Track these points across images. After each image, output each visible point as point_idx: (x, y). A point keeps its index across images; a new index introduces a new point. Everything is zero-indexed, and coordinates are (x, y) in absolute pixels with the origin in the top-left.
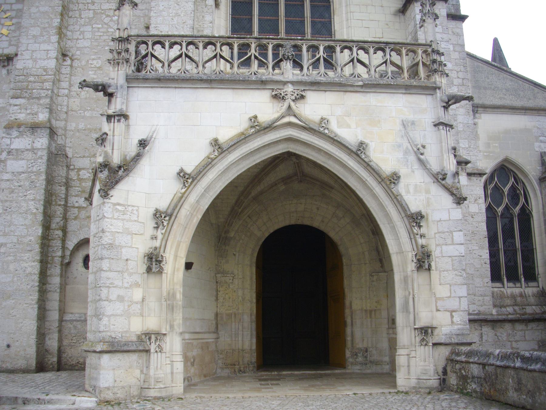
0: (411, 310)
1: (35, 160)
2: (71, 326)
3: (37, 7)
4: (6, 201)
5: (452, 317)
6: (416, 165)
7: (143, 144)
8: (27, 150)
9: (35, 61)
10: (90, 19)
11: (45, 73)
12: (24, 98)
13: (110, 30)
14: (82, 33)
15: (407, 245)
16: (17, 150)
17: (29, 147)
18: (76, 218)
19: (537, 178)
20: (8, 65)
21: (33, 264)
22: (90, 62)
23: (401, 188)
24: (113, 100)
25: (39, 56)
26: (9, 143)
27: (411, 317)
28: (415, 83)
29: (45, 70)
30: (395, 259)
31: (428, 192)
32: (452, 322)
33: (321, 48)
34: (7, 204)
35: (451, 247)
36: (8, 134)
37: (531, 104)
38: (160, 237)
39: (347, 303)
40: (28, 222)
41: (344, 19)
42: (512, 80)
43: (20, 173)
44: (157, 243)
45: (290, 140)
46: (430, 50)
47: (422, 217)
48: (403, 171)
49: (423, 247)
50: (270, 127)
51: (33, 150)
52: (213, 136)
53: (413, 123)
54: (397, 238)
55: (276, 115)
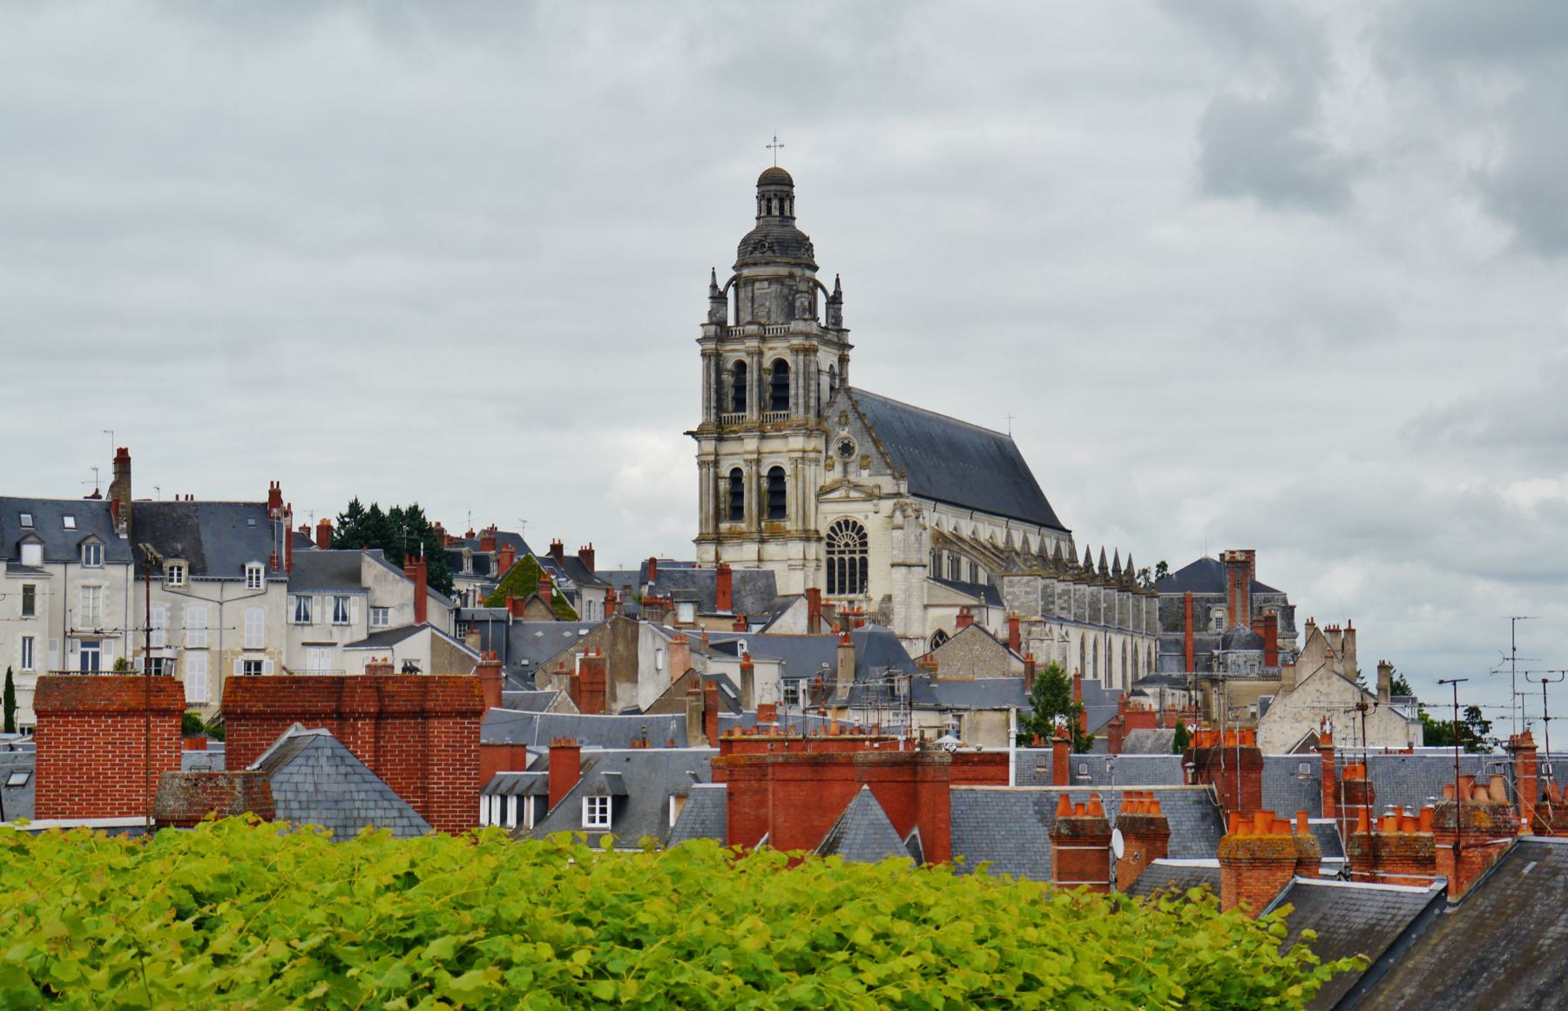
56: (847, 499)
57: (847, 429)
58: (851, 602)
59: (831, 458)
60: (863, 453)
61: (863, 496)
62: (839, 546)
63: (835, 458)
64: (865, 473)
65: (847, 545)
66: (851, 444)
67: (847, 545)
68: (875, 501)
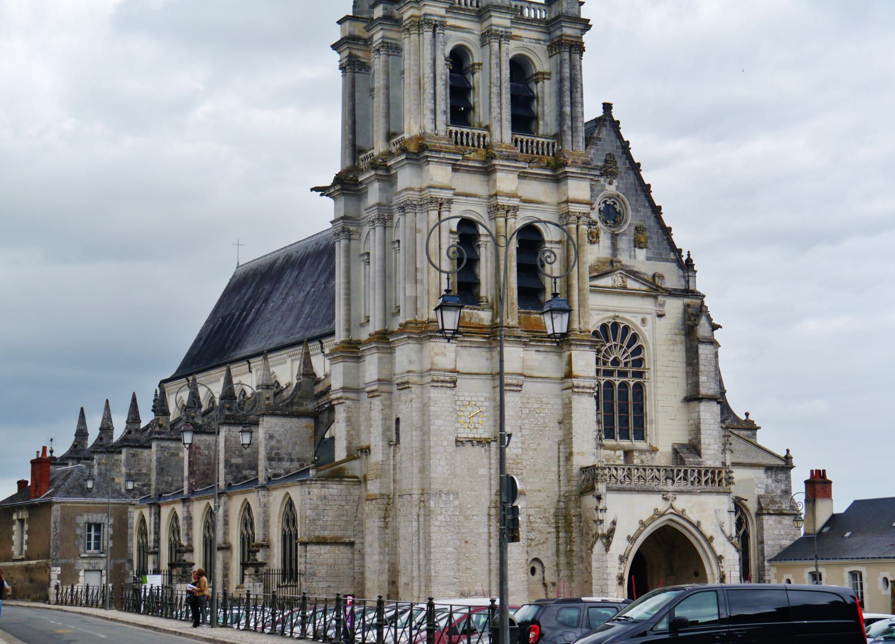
6: (720, 532)
7: (614, 523)
11: (517, 458)
13: (539, 423)
19: (755, 512)
22: (530, 445)
23: (714, 544)
24: (601, 501)
28: (721, 490)
29: (517, 456)
31: (724, 545)
33: (682, 471)
37: (754, 461)
38: (623, 568)
41: (653, 405)
42: (744, 444)
44: (622, 572)
45: (670, 520)
46: (728, 471)
47: (723, 558)
50: (662, 515)
52: (640, 519)
53: (719, 510)
55: (665, 508)
56: (623, 291)
57: (615, 182)
58: (628, 453)
60: (638, 223)
61: (645, 288)
62: (605, 363)
64: (641, 254)
65: (616, 362)
66: (618, 207)
67: (616, 362)
68: (661, 299)
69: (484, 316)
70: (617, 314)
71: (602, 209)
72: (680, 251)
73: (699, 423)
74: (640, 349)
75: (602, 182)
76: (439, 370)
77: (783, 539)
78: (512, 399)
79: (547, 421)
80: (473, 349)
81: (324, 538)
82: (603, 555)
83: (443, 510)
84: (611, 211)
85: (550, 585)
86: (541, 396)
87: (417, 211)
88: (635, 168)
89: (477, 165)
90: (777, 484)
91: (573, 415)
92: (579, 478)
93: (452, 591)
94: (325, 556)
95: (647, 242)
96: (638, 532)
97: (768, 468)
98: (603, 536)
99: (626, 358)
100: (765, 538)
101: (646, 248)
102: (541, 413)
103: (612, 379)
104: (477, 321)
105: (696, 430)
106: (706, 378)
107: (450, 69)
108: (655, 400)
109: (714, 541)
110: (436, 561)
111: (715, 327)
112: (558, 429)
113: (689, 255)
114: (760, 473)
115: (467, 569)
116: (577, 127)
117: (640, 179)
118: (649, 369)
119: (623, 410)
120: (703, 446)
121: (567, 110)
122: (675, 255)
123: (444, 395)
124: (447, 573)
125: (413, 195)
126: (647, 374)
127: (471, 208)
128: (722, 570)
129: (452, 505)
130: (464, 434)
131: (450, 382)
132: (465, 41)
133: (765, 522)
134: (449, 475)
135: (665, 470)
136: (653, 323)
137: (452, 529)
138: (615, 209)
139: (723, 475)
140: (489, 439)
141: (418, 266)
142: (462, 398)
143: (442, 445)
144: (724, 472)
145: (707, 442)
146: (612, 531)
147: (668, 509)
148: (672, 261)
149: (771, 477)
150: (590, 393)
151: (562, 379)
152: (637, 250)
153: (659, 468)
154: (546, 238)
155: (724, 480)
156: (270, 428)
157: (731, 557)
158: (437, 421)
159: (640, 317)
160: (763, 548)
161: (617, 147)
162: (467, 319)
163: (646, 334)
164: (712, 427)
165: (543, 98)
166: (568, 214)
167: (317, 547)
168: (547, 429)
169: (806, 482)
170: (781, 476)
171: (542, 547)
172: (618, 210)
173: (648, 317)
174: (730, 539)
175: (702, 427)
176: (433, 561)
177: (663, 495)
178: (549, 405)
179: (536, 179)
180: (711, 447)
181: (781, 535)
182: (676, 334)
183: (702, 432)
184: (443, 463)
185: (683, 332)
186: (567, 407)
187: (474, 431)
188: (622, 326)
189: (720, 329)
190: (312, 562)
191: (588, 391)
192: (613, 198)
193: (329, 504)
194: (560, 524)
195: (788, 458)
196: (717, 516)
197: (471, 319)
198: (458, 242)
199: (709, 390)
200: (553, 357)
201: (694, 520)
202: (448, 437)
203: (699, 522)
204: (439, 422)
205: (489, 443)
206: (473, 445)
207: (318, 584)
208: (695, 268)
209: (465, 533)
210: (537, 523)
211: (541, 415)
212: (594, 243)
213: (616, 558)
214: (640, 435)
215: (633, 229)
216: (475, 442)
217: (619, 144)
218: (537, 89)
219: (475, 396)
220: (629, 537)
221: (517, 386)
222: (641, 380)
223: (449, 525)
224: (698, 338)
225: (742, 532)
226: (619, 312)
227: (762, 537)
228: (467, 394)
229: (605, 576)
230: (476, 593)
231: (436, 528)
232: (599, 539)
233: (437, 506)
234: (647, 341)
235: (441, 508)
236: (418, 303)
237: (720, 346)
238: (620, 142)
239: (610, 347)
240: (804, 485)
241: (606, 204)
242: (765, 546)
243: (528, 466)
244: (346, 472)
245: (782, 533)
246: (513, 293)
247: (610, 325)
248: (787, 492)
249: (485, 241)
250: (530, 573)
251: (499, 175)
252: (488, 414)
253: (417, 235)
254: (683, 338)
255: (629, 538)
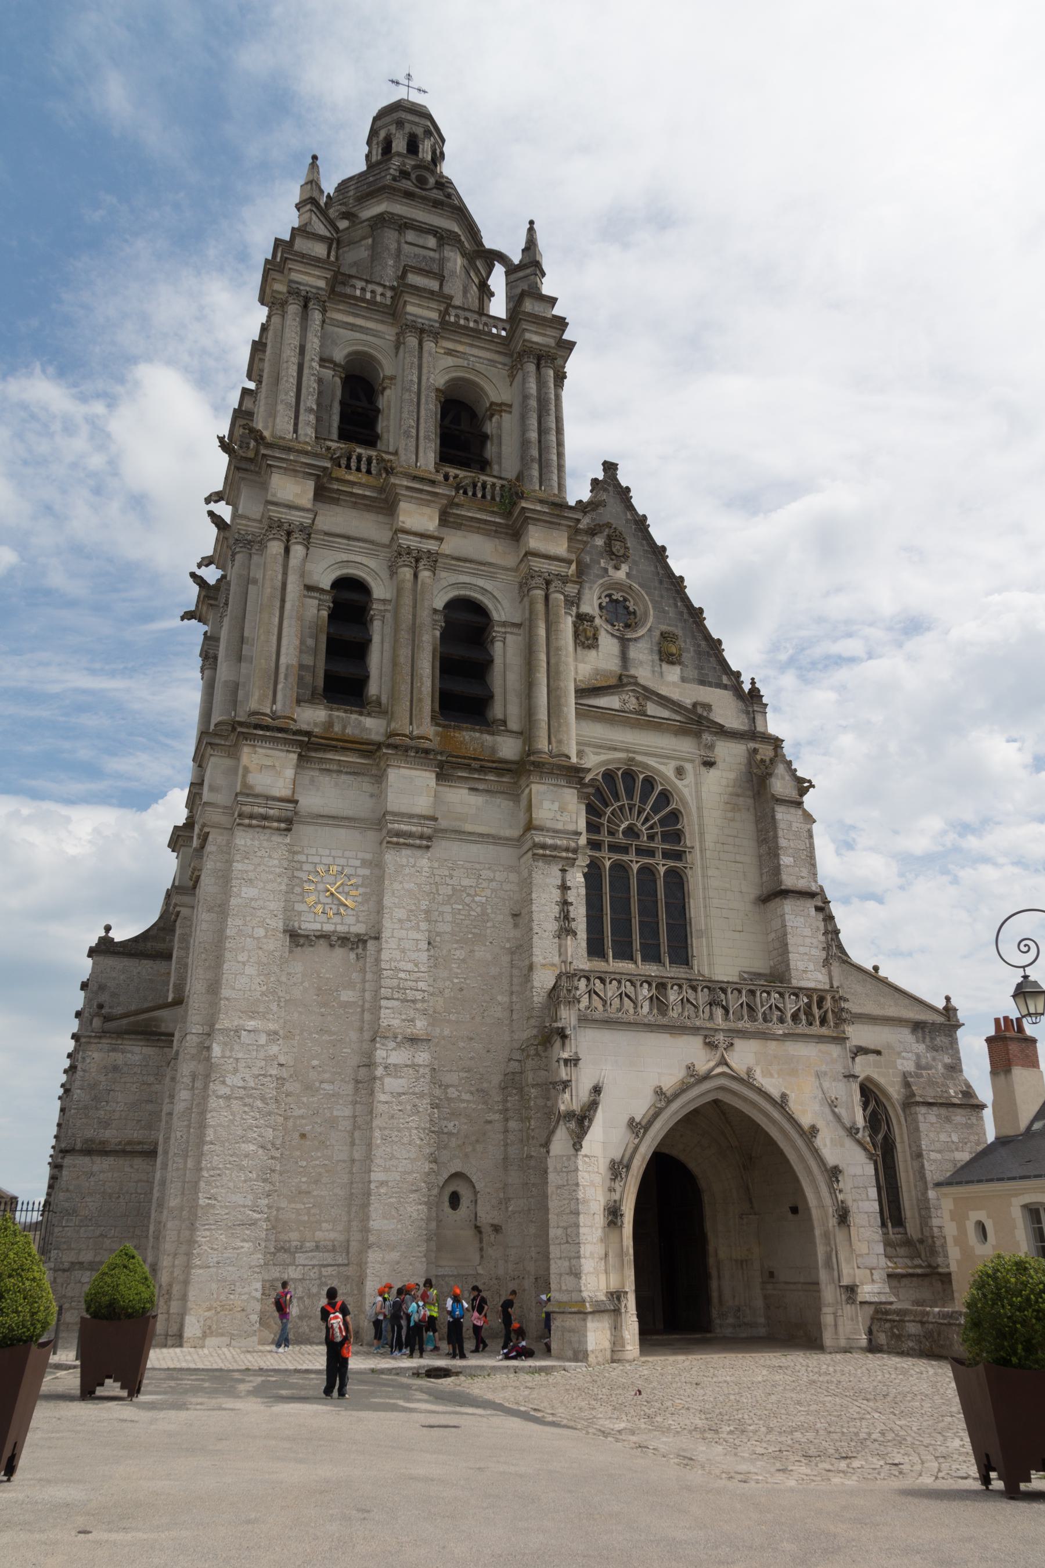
0: (835, 1267)
1: (417, 1079)
2: (443, 1283)
3: (401, 883)
4: (385, 1128)
5: (872, 1274)
7: (597, 1090)
8: (407, 1066)
9: (403, 951)
10: (450, 897)
12: (397, 999)
13: (472, 913)
14: (441, 913)
15: (828, 1201)
16: (395, 1065)
17: (409, 1063)
18: (445, 1147)
20: (358, 947)
21: (420, 1207)
22: (453, 952)
23: (819, 1142)
24: (567, 1042)
25: (407, 947)
26: (385, 1055)
27: (836, 1273)
30: (815, 1213)
31: (842, 1146)
32: (873, 1280)
34: (386, 1132)
35: (867, 1203)
36: (383, 1045)
38: (619, 1189)
39: (711, 1248)
40: (413, 1156)
43: (400, 1094)
44: (617, 1197)
45: (722, 1088)
46: (837, 996)
48: (820, 1125)
49: (842, 1202)
50: (707, 1077)
51: (413, 1066)
54: (817, 1192)
55: (712, 1064)
56: (641, 721)
57: (625, 568)
59: (591, 619)
61: (678, 718)
63: (598, 621)
64: (673, 673)
65: (630, 831)
68: (707, 737)
69: (372, 726)
70: (631, 755)
71: (604, 604)
72: (738, 674)
73: (785, 934)
74: (675, 816)
75: (603, 565)
76: (257, 796)
77: (957, 1149)
78: (412, 860)
79: (489, 911)
80: (343, 777)
81: (103, 1143)
82: (569, 1158)
83: (242, 1065)
84: (621, 611)
85: (490, 1229)
86: (477, 866)
87: (254, 551)
88: (659, 553)
89: (368, 493)
90: (935, 1053)
91: (534, 896)
92: (547, 1011)
93: (244, 1240)
94: (102, 1176)
95: (680, 655)
96: (651, 1112)
97: (918, 1027)
98: (570, 1115)
99: (651, 827)
100: (924, 1147)
101: (680, 663)
102: (476, 895)
103: (625, 858)
104: (357, 732)
105: (782, 948)
106: (791, 859)
107: (341, 378)
108: (704, 898)
109: (819, 1137)
110: (212, 1173)
111: (803, 786)
112: (511, 926)
113: (753, 683)
114: (905, 1035)
115: (300, 1193)
116: (548, 460)
117: (667, 568)
118: (693, 848)
119: (649, 910)
120: (793, 973)
121: (533, 435)
122: (730, 679)
123: (265, 844)
124: (238, 1199)
125: (246, 525)
126: (689, 857)
127: (358, 559)
128: (840, 1197)
129: (262, 1055)
130: (310, 924)
131: (279, 820)
132: (370, 347)
133: (921, 1118)
134: (263, 994)
135: (708, 988)
136: (695, 775)
137: (259, 1103)
138: (627, 608)
139: (828, 1004)
140: (365, 935)
141: (246, 634)
142: (316, 859)
143: (251, 936)
144: (829, 998)
145: (801, 966)
146: (592, 1106)
147: (717, 1065)
148: (725, 687)
149: (924, 1042)
150: (567, 858)
151: (518, 840)
152: (665, 666)
153: (695, 983)
154: (495, 616)
155: (830, 1015)
156: (102, 972)
157: (858, 1171)
158: (244, 889)
159: (673, 764)
160: (922, 1166)
161: (627, 521)
162: (337, 728)
163: (686, 791)
164: (808, 941)
165: (500, 437)
166: (531, 575)
167: (87, 1160)
168: (489, 924)
169: (989, 1040)
170: (941, 1040)
171: (474, 1150)
172: (631, 609)
173: (688, 766)
174: (852, 1131)
175: (791, 940)
176: (205, 1174)
177: (706, 1037)
178: (494, 883)
179: (478, 531)
180: (809, 975)
181: (953, 1142)
182: (738, 795)
183: (791, 949)
184: (250, 970)
185: (749, 793)
186: (526, 885)
187: (337, 919)
188: (641, 777)
189: (811, 790)
190: (71, 1188)
191: (564, 854)
192: (623, 591)
193: (123, 1080)
194: (509, 1105)
195: (949, 1011)
196: (821, 1084)
197: (344, 727)
198: (329, 607)
199: (797, 879)
200: (503, 804)
201: (776, 1094)
202: (268, 920)
203: (784, 1096)
204: (248, 892)
205: (365, 942)
206: (332, 946)
207: (78, 1232)
208: (765, 700)
209: (302, 1117)
210: (463, 1101)
211: (477, 899)
212: (589, 647)
213: (602, 1166)
214: (681, 954)
215: (657, 633)
216: (334, 938)
217: (629, 517)
218: (489, 428)
219: (343, 857)
220: (632, 1120)
221: (421, 837)
222: (679, 864)
223: (250, 1096)
224: (773, 795)
225: (880, 1136)
226: (634, 752)
227: (919, 1146)
228: (327, 852)
229: (573, 1206)
230: (317, 1247)
231: (221, 1101)
232: (561, 1123)
233: (228, 1054)
234: (687, 803)
235: (237, 1059)
236: (241, 693)
237: (814, 821)
238: (632, 515)
239: (621, 808)
240: (985, 1045)
241: (612, 601)
242: (926, 1163)
243: (447, 991)
244: (163, 1025)
245: (955, 1138)
246: (422, 684)
247: (620, 773)
248: (955, 1068)
249: (380, 610)
250: (447, 1204)
251: (403, 505)
252: (368, 890)
253: (250, 586)
254: (750, 801)
255: (632, 1124)
